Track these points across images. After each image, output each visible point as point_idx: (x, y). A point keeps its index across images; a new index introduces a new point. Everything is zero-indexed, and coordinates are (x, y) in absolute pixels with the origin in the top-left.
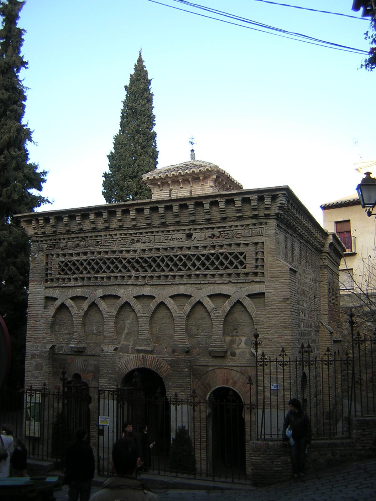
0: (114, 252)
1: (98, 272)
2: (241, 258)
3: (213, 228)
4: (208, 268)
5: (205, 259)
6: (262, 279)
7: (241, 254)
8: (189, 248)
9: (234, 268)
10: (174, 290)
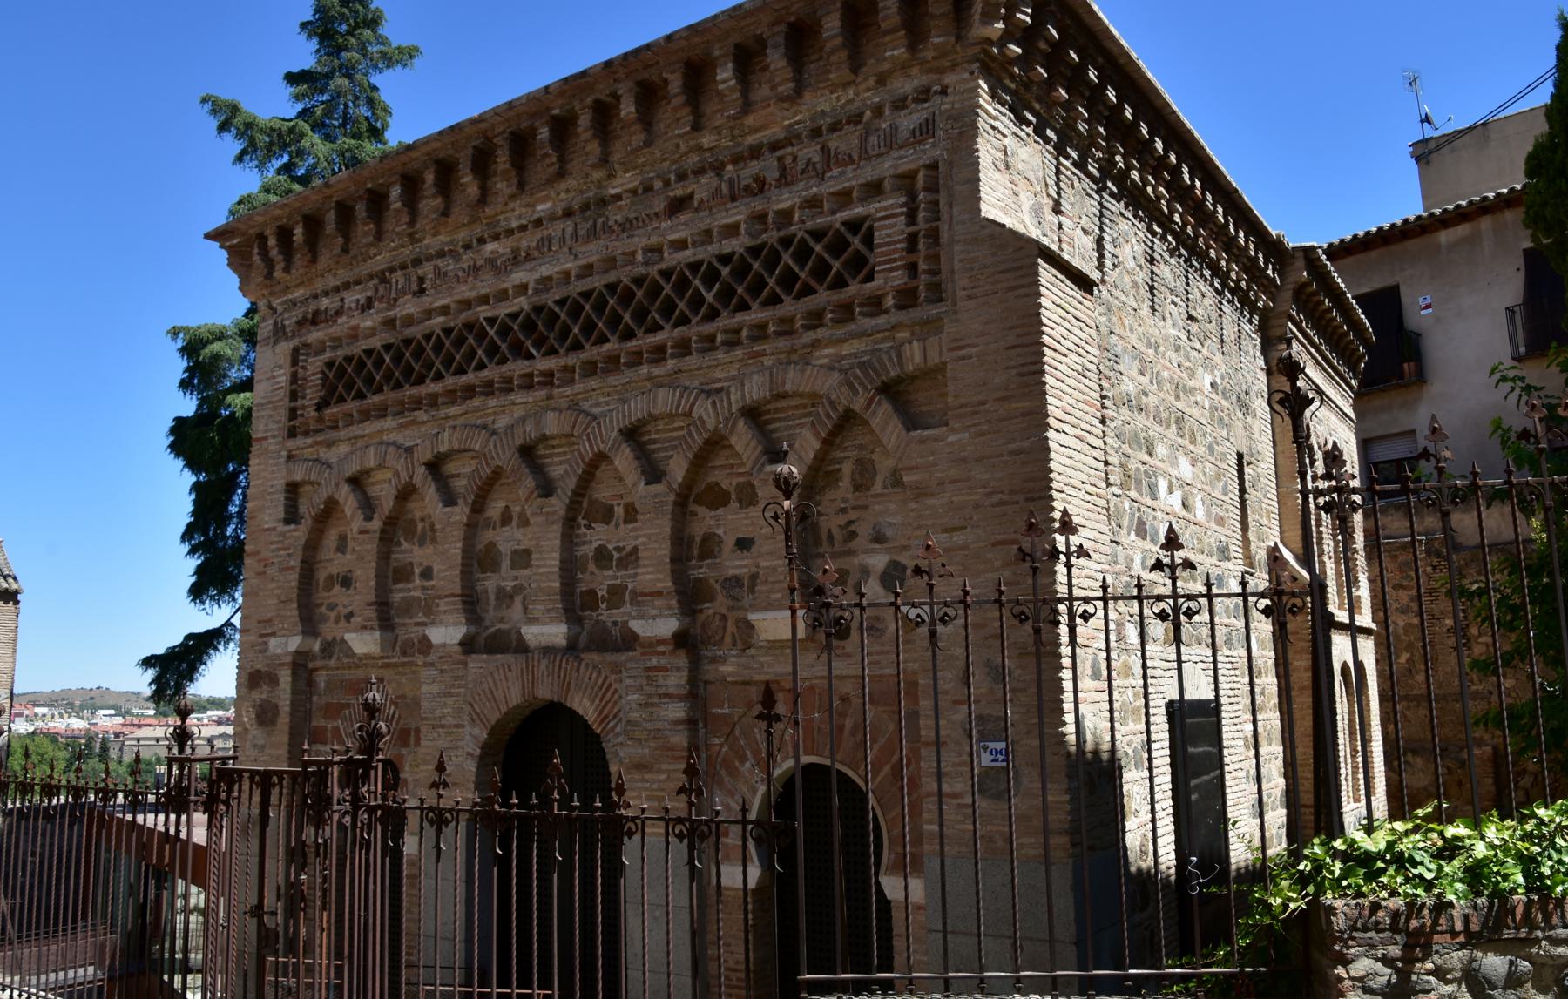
0: (467, 304)
1: (420, 381)
2: (856, 242)
3: (755, 152)
4: (744, 307)
5: (732, 273)
6: (934, 310)
7: (854, 226)
8: (681, 245)
9: (830, 288)
10: (637, 408)
